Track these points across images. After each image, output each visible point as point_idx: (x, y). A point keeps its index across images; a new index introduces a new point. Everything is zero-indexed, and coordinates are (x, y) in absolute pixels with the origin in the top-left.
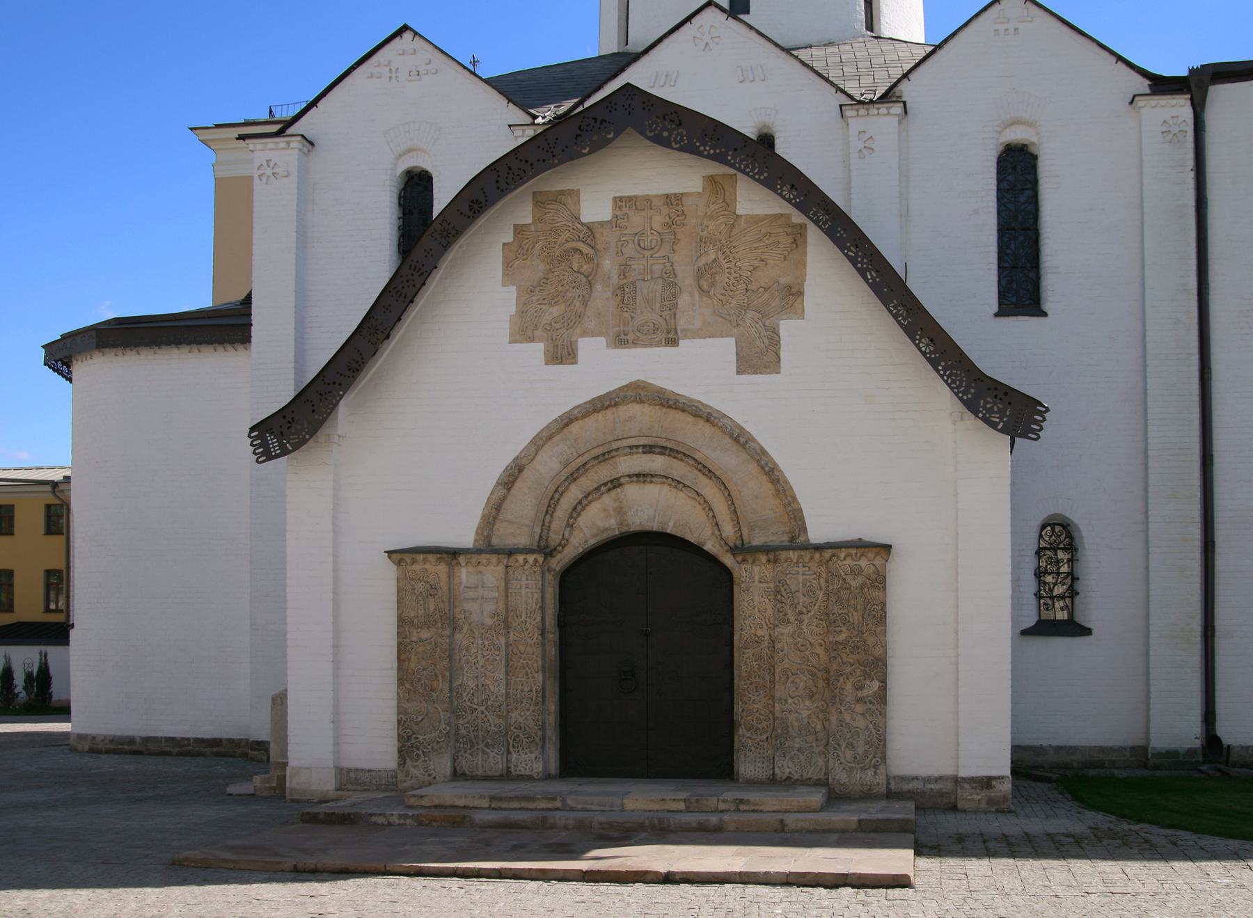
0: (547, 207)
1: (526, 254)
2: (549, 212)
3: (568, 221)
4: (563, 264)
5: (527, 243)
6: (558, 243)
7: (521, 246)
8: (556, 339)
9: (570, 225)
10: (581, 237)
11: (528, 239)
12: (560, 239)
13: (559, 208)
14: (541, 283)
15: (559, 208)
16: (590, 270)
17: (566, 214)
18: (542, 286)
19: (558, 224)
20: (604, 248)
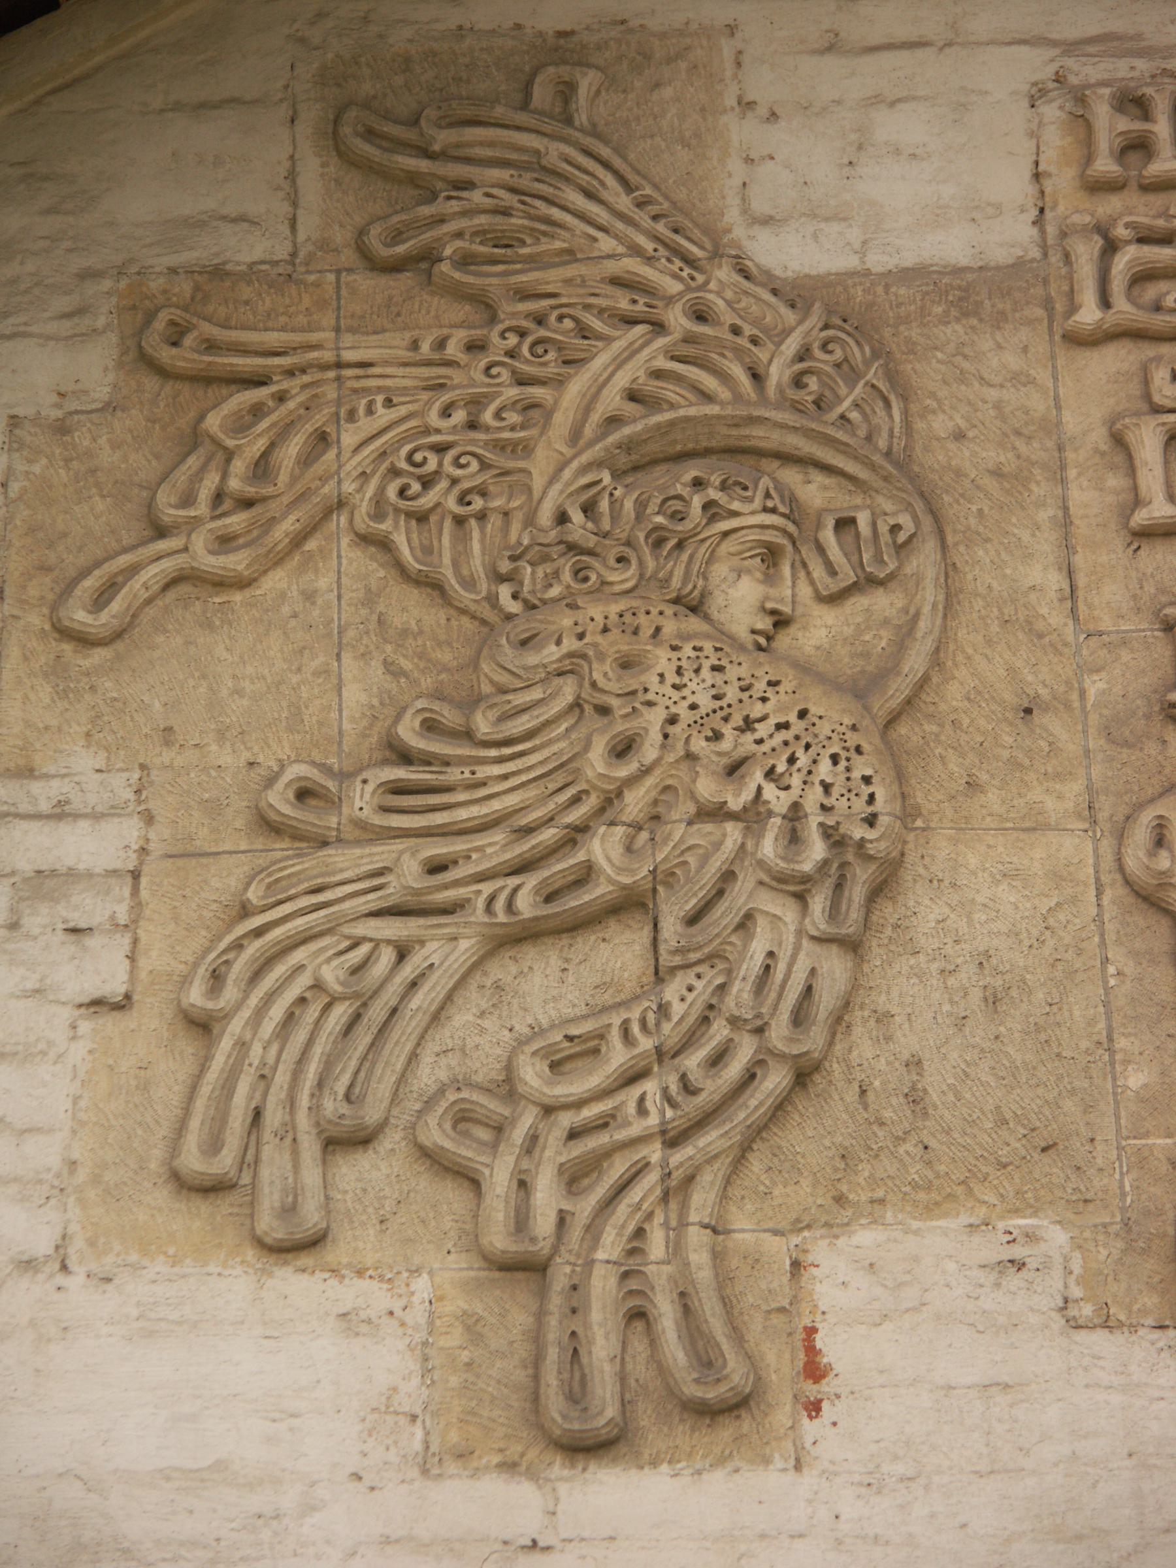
0: (442, 138)
1: (248, 503)
2: (469, 185)
3: (649, 260)
4: (623, 578)
5: (258, 411)
6: (562, 421)
7: (194, 439)
8: (562, 1220)
9: (675, 287)
10: (778, 373)
11: (260, 381)
12: (576, 387)
13: (554, 152)
14: (409, 733)
15: (554, 152)
16: (883, 640)
17: (624, 202)
18: (405, 757)
19: (551, 279)
20: (997, 473)
